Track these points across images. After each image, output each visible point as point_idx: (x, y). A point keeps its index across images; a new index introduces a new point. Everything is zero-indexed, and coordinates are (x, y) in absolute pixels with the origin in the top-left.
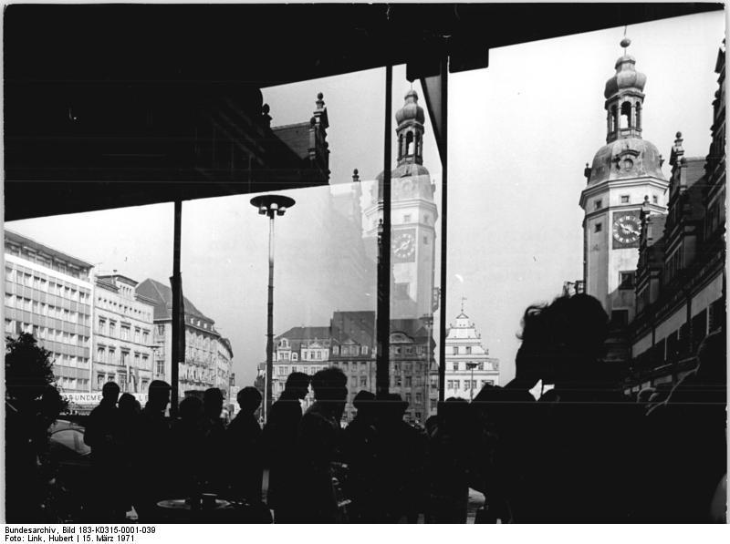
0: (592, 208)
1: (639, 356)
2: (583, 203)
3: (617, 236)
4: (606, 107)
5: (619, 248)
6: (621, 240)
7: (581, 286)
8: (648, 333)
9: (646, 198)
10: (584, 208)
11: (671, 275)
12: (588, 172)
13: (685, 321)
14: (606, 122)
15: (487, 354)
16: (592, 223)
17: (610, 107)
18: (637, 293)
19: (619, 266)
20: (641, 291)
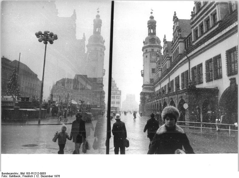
0: (145, 51)
2: (143, 50)
7: (143, 71)
9: (158, 50)
12: (144, 42)
13: (168, 82)
14: (148, 31)
20: (157, 74)
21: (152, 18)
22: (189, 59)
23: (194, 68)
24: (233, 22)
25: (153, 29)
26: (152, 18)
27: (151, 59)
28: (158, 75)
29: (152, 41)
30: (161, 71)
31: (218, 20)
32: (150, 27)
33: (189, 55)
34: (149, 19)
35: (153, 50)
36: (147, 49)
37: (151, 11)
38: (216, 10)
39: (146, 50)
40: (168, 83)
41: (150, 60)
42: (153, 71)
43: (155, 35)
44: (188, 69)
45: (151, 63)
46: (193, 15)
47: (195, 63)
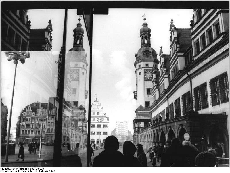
1: (154, 117)
4: (141, 37)
7: (136, 92)
13: (167, 106)
15: (105, 115)
16: (138, 72)
17: (142, 37)
22: (190, 78)
23: (197, 89)
24: (227, 42)
25: (147, 40)
27: (145, 77)
28: (155, 97)
29: (146, 53)
30: (158, 92)
31: (221, 32)
32: (143, 37)
33: (190, 73)
34: (142, 27)
35: (147, 65)
37: (144, 18)
38: (218, 20)
39: (140, 66)
40: (167, 108)
41: (145, 78)
42: (149, 91)
44: (190, 90)
45: (146, 82)
46: (193, 24)
47: (197, 81)
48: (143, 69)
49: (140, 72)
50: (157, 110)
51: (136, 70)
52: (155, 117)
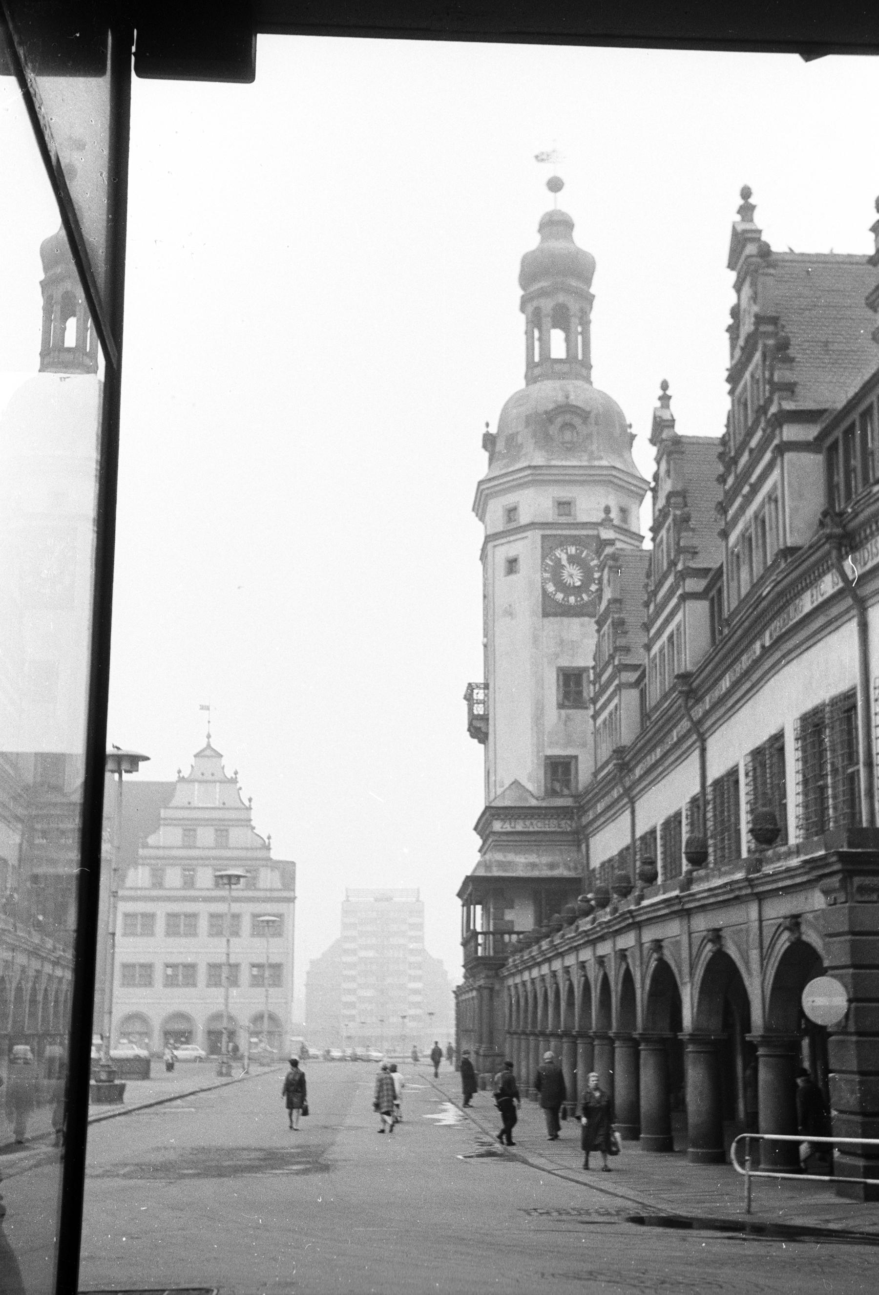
1: (603, 865)
2: (480, 508)
3: (551, 588)
4: (523, 309)
5: (555, 615)
6: (560, 596)
7: (479, 694)
8: (622, 810)
9: (607, 510)
10: (482, 519)
11: (662, 683)
12: (489, 441)
13: (696, 789)
16: (502, 552)
17: (530, 308)
18: (594, 717)
19: (557, 656)
20: (605, 714)
21: (556, 225)
25: (566, 329)
26: (556, 225)
28: (612, 724)
29: (557, 424)
30: (635, 693)
36: (510, 499)
39: (511, 512)
40: (694, 801)
43: (588, 380)
48: (535, 536)
49: (512, 554)
50: (625, 818)
51: (486, 543)
52: (610, 860)
